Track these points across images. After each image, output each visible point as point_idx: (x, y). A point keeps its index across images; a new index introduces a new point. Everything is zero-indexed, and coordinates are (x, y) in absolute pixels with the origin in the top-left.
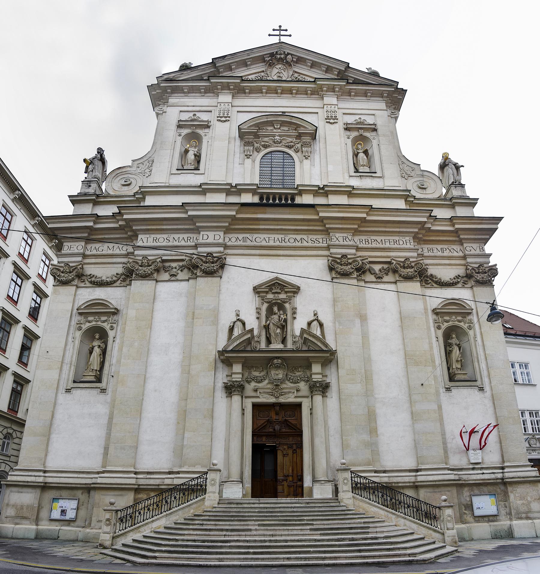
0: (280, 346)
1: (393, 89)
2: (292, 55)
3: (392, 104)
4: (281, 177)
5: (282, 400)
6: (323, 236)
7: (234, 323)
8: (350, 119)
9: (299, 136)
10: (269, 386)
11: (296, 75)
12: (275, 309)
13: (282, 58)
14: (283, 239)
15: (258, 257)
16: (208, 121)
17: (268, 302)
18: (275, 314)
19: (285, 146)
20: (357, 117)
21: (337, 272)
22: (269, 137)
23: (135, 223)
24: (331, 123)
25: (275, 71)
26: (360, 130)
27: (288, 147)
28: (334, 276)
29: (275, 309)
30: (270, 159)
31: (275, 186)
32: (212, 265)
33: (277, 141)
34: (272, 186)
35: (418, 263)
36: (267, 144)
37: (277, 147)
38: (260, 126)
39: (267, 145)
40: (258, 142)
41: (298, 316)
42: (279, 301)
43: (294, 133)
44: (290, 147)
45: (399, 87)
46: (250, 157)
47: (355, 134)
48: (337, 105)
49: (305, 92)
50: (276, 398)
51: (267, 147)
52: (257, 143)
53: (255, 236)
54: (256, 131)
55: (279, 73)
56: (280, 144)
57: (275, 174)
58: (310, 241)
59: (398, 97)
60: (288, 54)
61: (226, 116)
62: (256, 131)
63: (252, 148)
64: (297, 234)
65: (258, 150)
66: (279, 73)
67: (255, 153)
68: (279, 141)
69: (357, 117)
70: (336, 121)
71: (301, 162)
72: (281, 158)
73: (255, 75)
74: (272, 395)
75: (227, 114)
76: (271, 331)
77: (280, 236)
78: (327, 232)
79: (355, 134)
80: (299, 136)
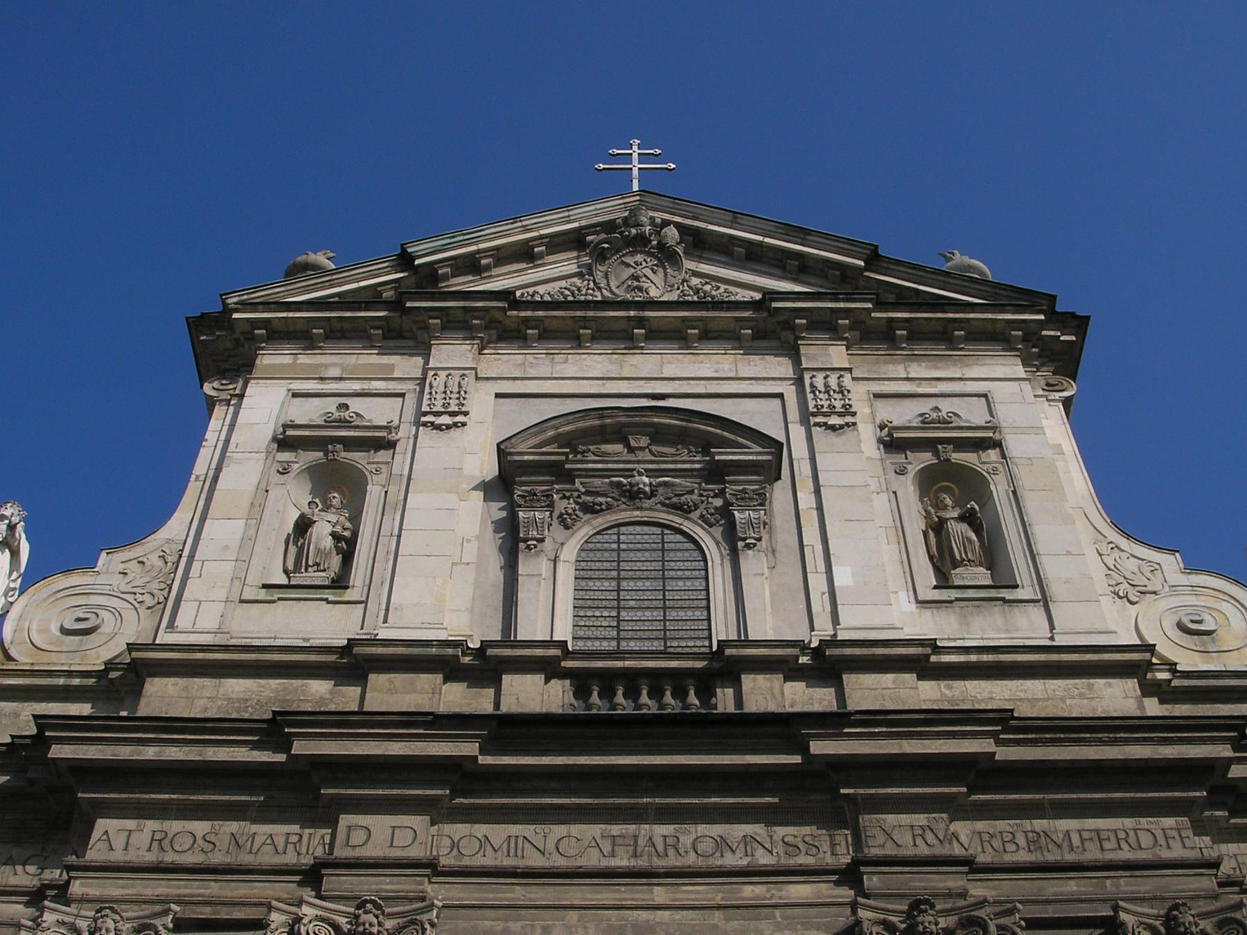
1: (1042, 317)
3: (1046, 360)
4: (655, 613)
8: (903, 414)
9: (716, 473)
16: (388, 428)
20: (925, 406)
22: (609, 477)
24: (833, 428)
26: (940, 447)
30: (613, 550)
31: (632, 644)
34: (623, 644)
36: (601, 499)
38: (570, 441)
39: (601, 504)
40: (568, 494)
44: (684, 510)
45: (1058, 308)
46: (539, 545)
47: (921, 460)
48: (850, 370)
51: (602, 510)
52: (564, 497)
54: (563, 458)
57: (632, 603)
59: (1062, 338)
61: (456, 409)
62: (563, 458)
63: (548, 513)
65: (567, 523)
67: (557, 531)
68: (647, 489)
69: (925, 406)
70: (849, 419)
72: (655, 545)
73: (563, 283)
75: (458, 405)
79: (921, 460)
80: (716, 473)
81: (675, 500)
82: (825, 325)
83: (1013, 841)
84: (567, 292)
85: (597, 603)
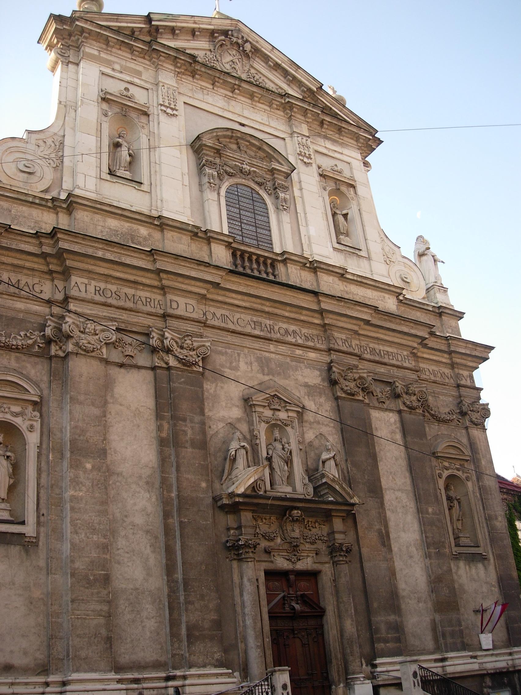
0: (289, 489)
2: (250, 43)
7: (236, 450)
11: (253, 71)
13: (237, 43)
14: (272, 327)
23: (71, 256)
25: (227, 58)
27: (258, 184)
29: (277, 434)
32: (191, 353)
35: (421, 391)
42: (279, 423)
44: (260, 184)
53: (237, 316)
55: (233, 62)
60: (247, 41)
76: (275, 465)
82: (305, 112)
83: (366, 350)
84: (207, 59)
85: (233, 218)
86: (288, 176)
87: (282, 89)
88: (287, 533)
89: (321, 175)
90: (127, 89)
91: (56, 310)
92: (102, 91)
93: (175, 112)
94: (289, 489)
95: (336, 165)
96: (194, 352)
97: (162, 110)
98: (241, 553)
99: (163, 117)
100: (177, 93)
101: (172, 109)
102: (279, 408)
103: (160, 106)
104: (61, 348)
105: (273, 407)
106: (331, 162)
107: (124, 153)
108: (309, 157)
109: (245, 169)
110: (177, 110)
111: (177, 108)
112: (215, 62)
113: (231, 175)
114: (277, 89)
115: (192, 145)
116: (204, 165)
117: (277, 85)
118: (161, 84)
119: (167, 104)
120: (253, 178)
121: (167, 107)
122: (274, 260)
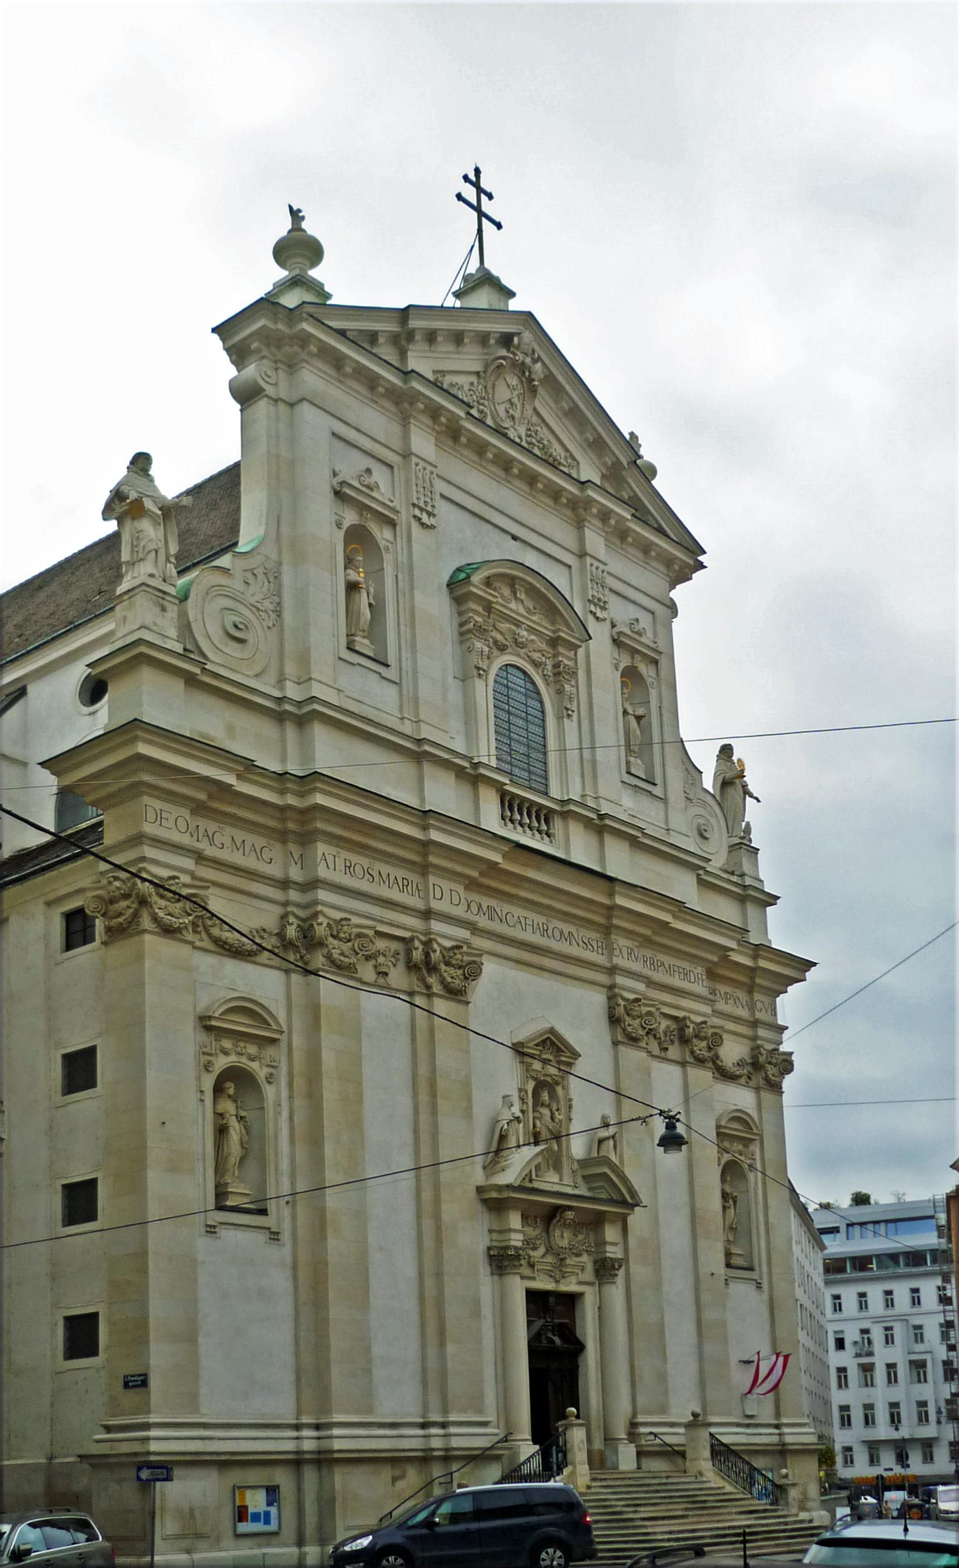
5: (563, 1288)
6: (598, 935)
9: (554, 642)
10: (550, 1259)
11: (535, 419)
12: (545, 1096)
15: (510, 963)
17: (535, 1079)
18: (542, 1105)
19: (529, 657)
21: (624, 1030)
27: (536, 665)
28: (620, 1038)
29: (545, 1096)
33: (522, 643)
37: (519, 655)
41: (573, 1115)
42: (549, 1079)
43: (546, 629)
49: (555, 494)
50: (557, 1282)
55: (512, 404)
56: (522, 648)
58: (581, 943)
64: (564, 921)
66: (512, 404)
71: (559, 718)
74: (551, 1276)
77: (539, 919)
78: (607, 930)
81: (536, 656)
86: (575, 647)
87: (574, 459)
88: (554, 1240)
89: (614, 641)
90: (368, 471)
91: (294, 895)
92: (335, 474)
93: (432, 521)
94: (555, 1178)
95: (637, 620)
96: (460, 972)
97: (415, 517)
98: (506, 1266)
99: (415, 528)
100: (435, 476)
101: (430, 514)
102: (551, 1058)
103: (412, 508)
104: (302, 957)
105: (544, 1056)
106: (633, 612)
107: (363, 600)
108: (604, 609)
109: (522, 637)
110: (434, 515)
111: (435, 513)
112: (486, 402)
113: (502, 648)
114: (566, 458)
115: (452, 585)
116: (469, 631)
117: (567, 450)
118: (414, 460)
119: (422, 505)
120: (529, 654)
121: (421, 509)
122: (551, 811)
